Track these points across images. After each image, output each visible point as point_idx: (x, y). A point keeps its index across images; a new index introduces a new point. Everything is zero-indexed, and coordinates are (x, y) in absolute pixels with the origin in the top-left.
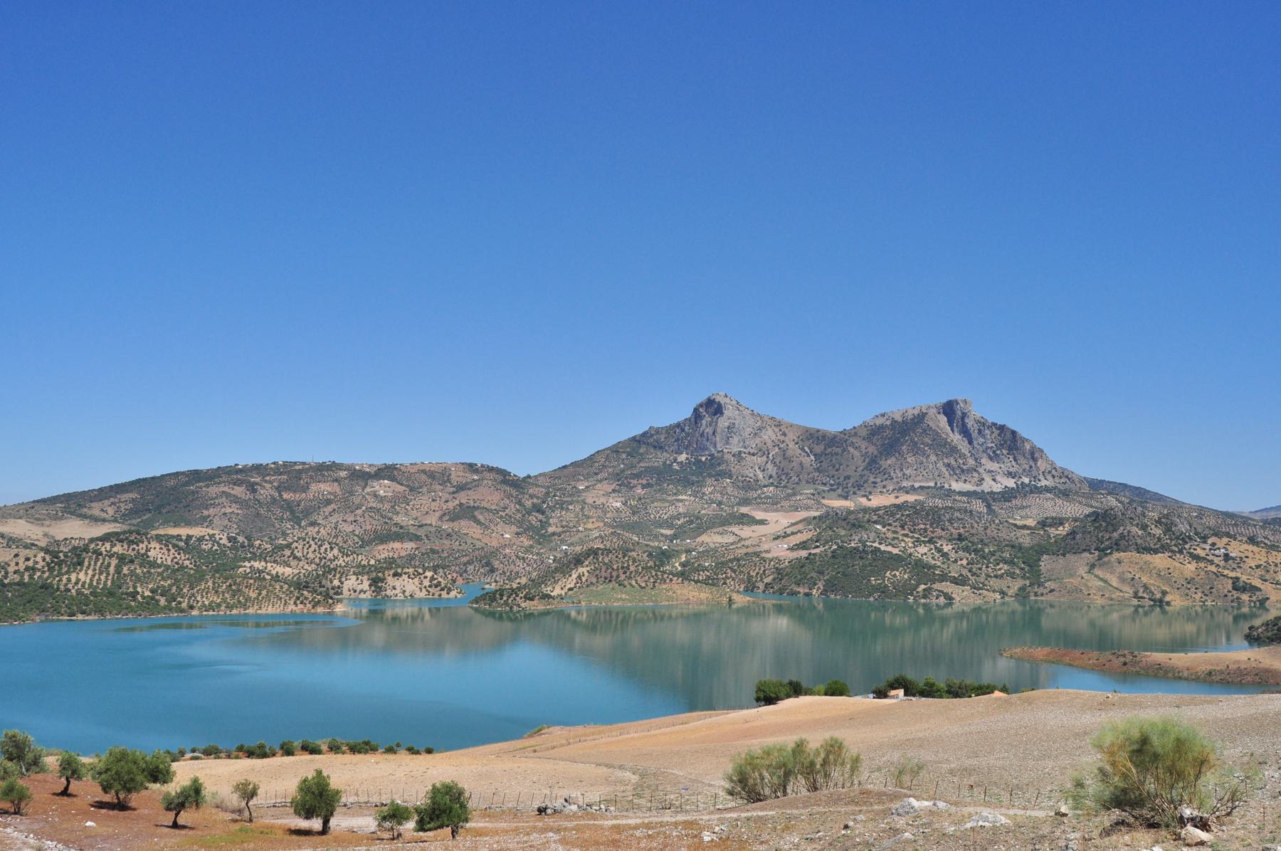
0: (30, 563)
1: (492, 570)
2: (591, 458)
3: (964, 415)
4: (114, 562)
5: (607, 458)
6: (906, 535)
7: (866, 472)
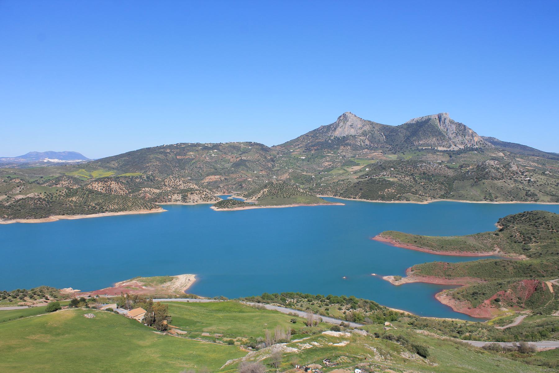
0: (61, 193)
1: (242, 187)
2: (297, 138)
3: (445, 119)
4: (87, 192)
5: (304, 138)
6: (403, 172)
7: (405, 143)
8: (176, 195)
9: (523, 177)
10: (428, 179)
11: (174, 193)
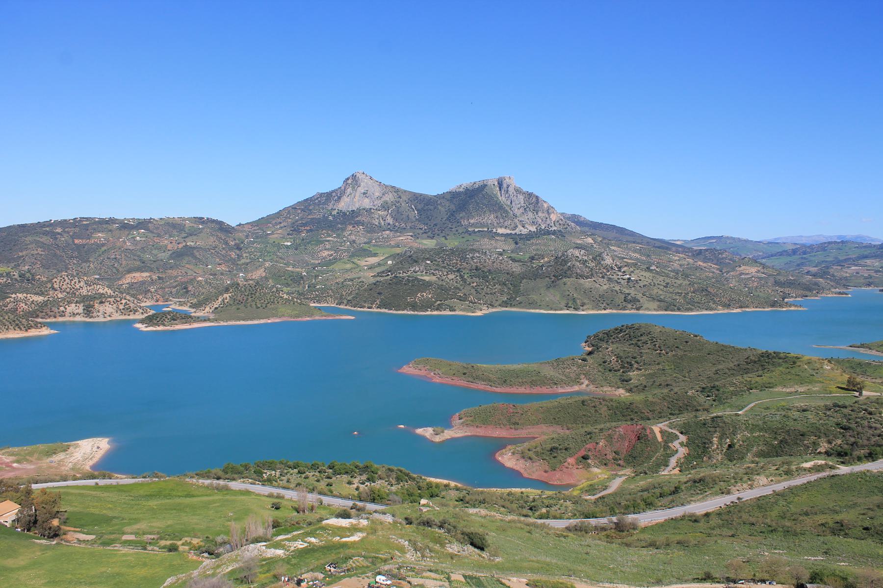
1: (187, 292)
2: (278, 213)
3: (508, 186)
6: (445, 267)
8: (73, 305)
9: (620, 274)
10: (483, 278)
11: (69, 303)
